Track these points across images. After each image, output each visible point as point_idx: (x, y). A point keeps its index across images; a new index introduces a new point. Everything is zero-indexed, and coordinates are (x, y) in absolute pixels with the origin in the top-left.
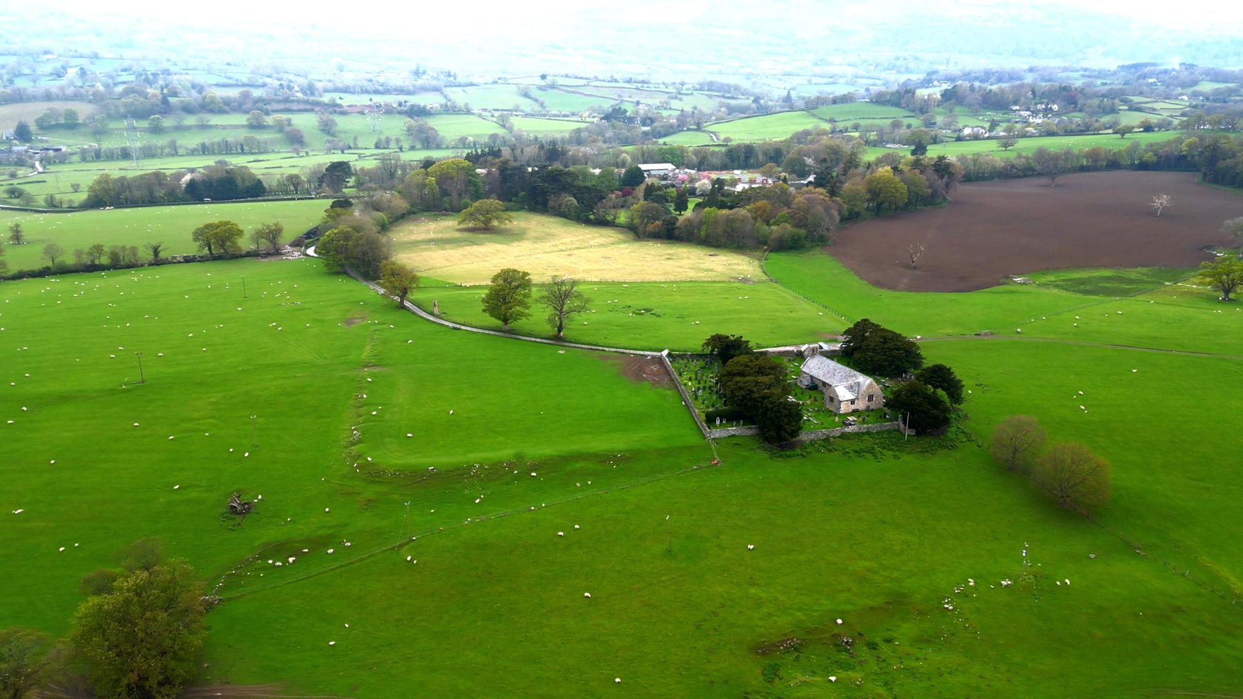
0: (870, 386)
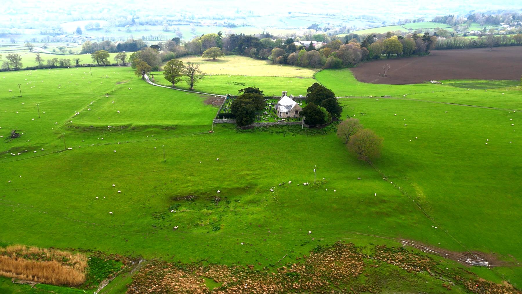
0: (296, 106)
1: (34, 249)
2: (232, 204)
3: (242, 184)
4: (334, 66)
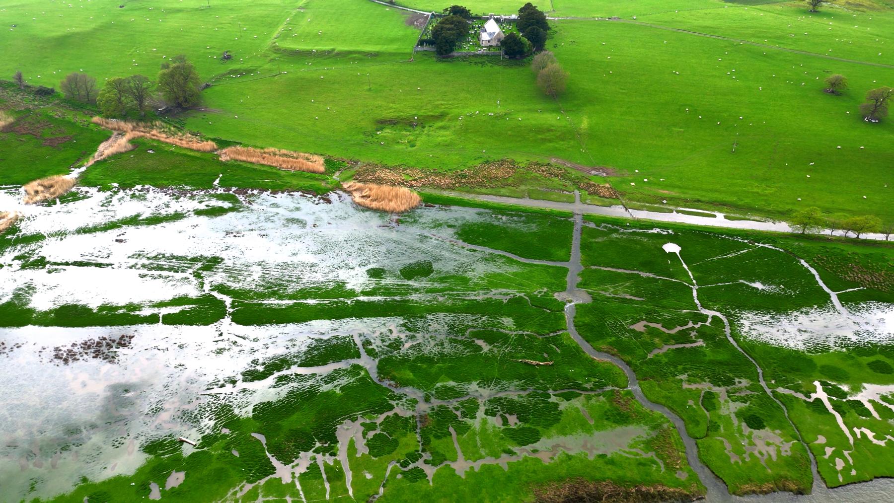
0: (499, 34)
1: (284, 151)
2: (427, 128)
3: (437, 112)
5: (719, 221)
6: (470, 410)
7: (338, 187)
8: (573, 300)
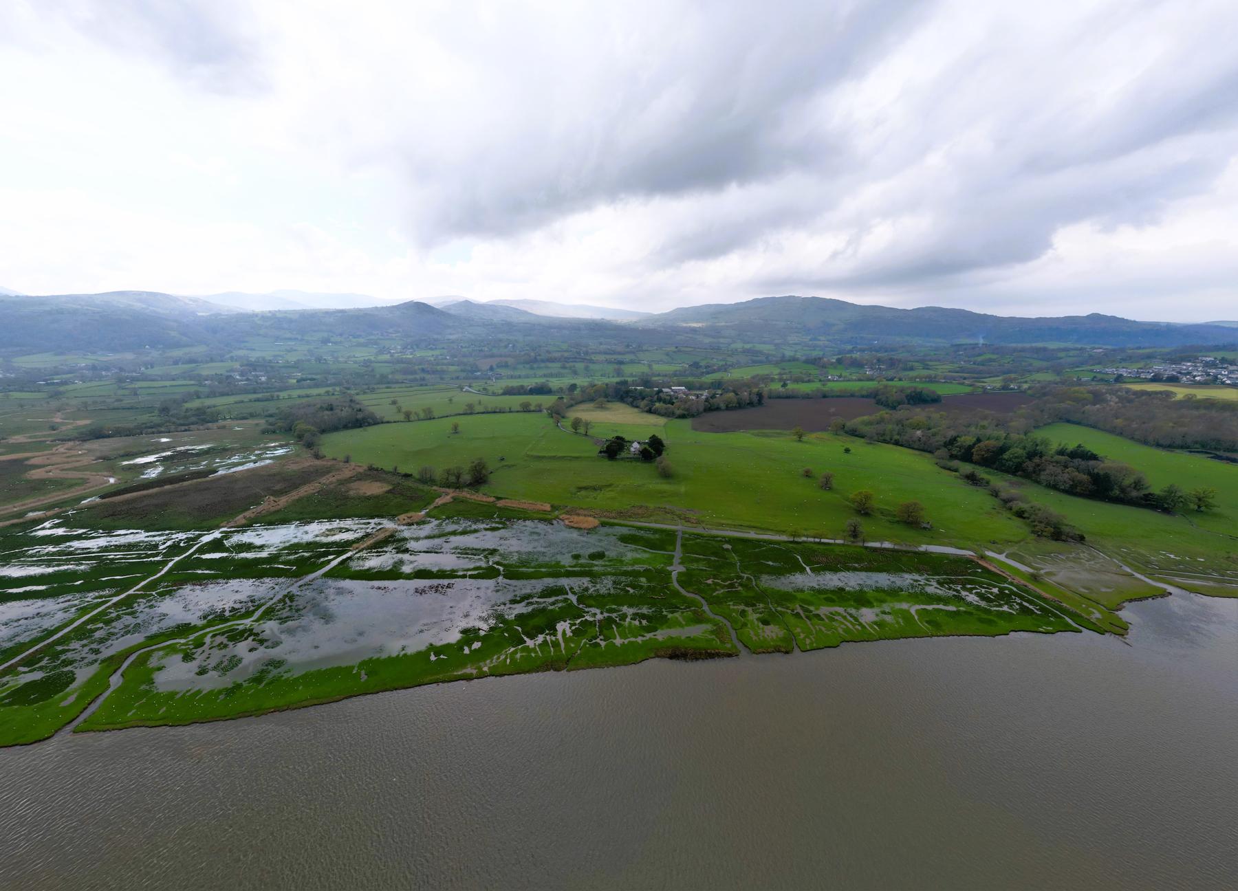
4: (682, 417)
5: (752, 535)
6: (624, 617)
7: (557, 517)
8: (676, 569)
